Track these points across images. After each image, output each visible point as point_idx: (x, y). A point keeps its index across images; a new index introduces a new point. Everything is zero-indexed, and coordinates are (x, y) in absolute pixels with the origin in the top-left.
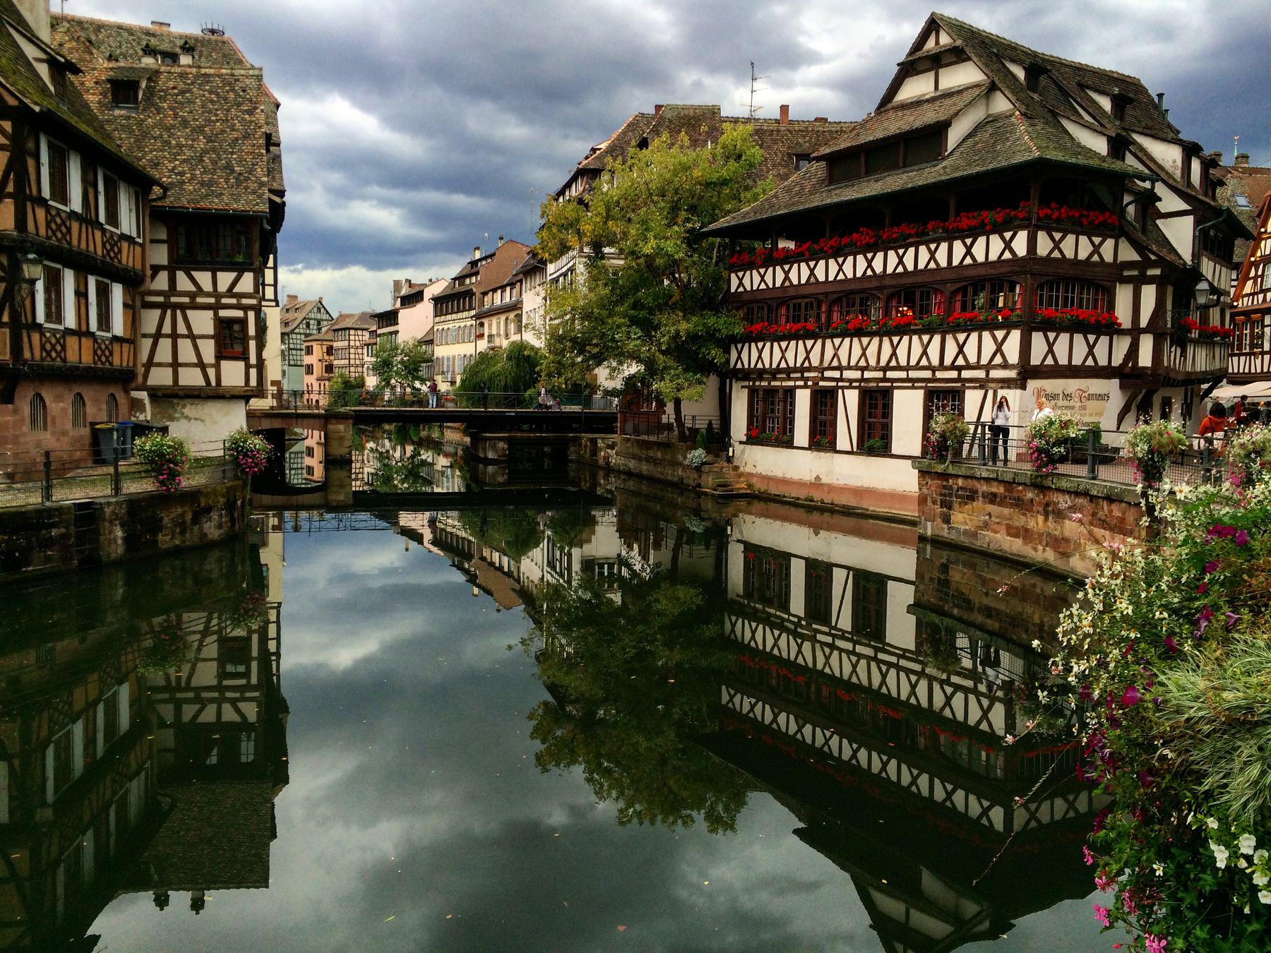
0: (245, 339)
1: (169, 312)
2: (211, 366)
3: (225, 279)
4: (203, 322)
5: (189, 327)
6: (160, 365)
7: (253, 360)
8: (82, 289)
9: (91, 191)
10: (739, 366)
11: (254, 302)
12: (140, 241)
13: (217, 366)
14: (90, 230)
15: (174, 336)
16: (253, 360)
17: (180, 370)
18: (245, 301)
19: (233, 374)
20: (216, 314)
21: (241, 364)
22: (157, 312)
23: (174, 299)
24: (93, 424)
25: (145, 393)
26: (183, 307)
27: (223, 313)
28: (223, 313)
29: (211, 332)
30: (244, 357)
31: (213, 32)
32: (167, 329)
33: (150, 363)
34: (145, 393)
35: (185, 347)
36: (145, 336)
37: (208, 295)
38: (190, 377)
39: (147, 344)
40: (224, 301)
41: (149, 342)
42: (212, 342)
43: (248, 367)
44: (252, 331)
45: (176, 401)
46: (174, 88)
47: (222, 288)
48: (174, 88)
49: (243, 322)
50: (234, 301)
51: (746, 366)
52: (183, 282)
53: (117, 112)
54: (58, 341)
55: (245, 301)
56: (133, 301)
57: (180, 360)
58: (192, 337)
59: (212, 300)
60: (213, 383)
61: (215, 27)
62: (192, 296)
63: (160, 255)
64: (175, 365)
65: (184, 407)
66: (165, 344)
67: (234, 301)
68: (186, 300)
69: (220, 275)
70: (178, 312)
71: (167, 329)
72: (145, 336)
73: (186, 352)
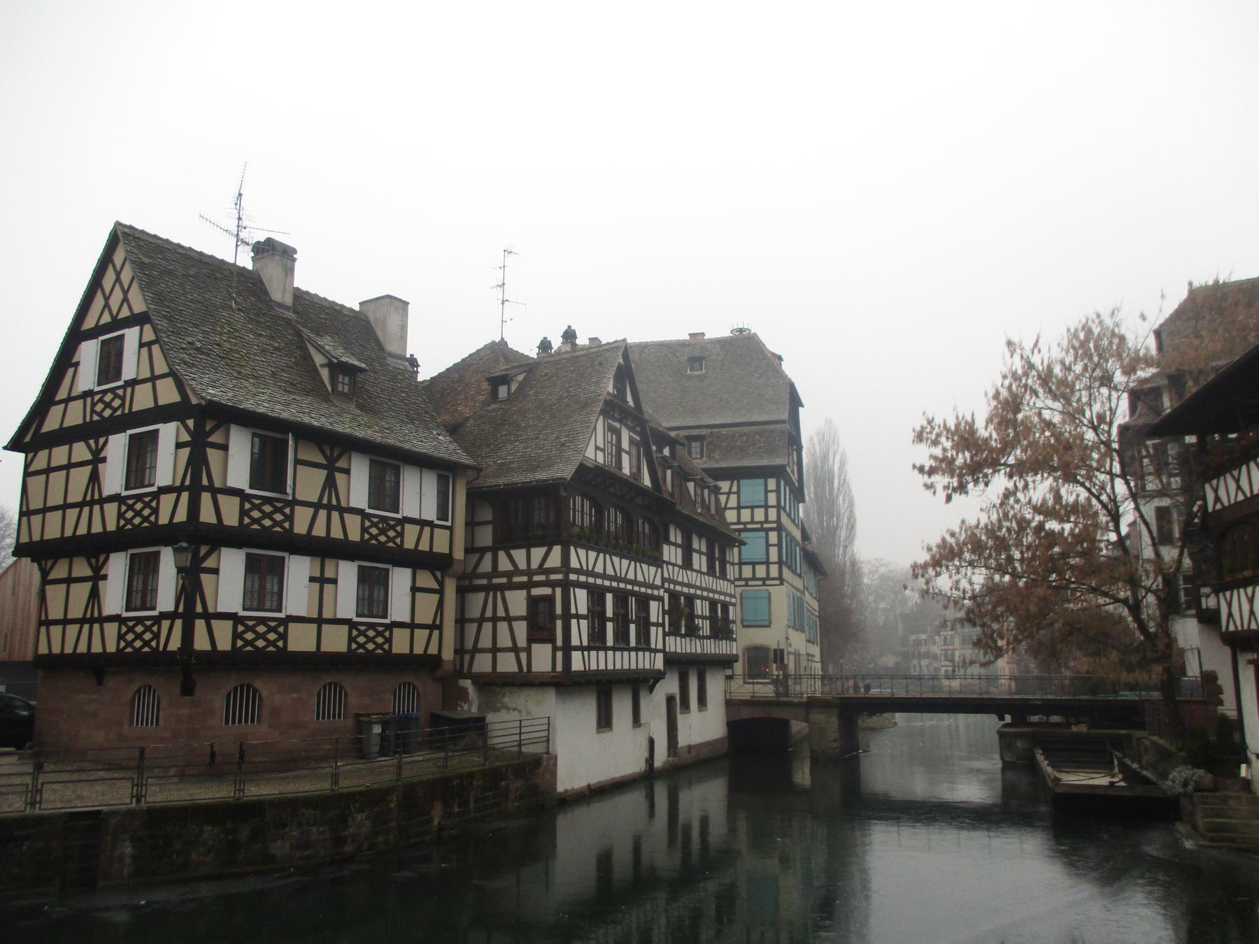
0: (553, 617)
1: (491, 593)
2: (523, 649)
3: (538, 553)
4: (517, 602)
5: (506, 610)
6: (483, 651)
7: (559, 643)
8: (329, 574)
9: (340, 478)
10: (1232, 628)
11: (559, 577)
12: (449, 524)
13: (528, 650)
14: (335, 515)
15: (495, 619)
16: (559, 643)
17: (499, 655)
18: (553, 577)
19: (542, 659)
20: (529, 593)
21: (549, 647)
22: (482, 595)
23: (496, 581)
24: (357, 716)
25: (469, 682)
26: (502, 588)
27: (536, 592)
28: (536, 592)
29: (524, 613)
30: (551, 639)
31: (741, 331)
32: (489, 613)
33: (476, 650)
34: (469, 682)
35: (503, 627)
36: (472, 621)
37: (522, 573)
38: (507, 664)
39: (471, 629)
40: (536, 578)
41: (474, 626)
42: (524, 623)
43: (555, 649)
44: (559, 610)
45: (498, 689)
46: (546, 375)
47: (535, 564)
48: (546, 375)
49: (550, 599)
50: (542, 578)
51: (1240, 628)
52: (504, 564)
53: (493, 406)
54: (131, 629)
55: (553, 577)
56: (441, 584)
57: (498, 646)
58: (509, 619)
59: (525, 579)
60: (525, 669)
61: (741, 326)
62: (508, 574)
63: (485, 537)
64: (495, 650)
65: (504, 695)
66: (488, 627)
67: (542, 578)
68: (504, 580)
69: (428, 549)
70: (499, 593)
71: (489, 613)
72: (472, 621)
73: (504, 640)
